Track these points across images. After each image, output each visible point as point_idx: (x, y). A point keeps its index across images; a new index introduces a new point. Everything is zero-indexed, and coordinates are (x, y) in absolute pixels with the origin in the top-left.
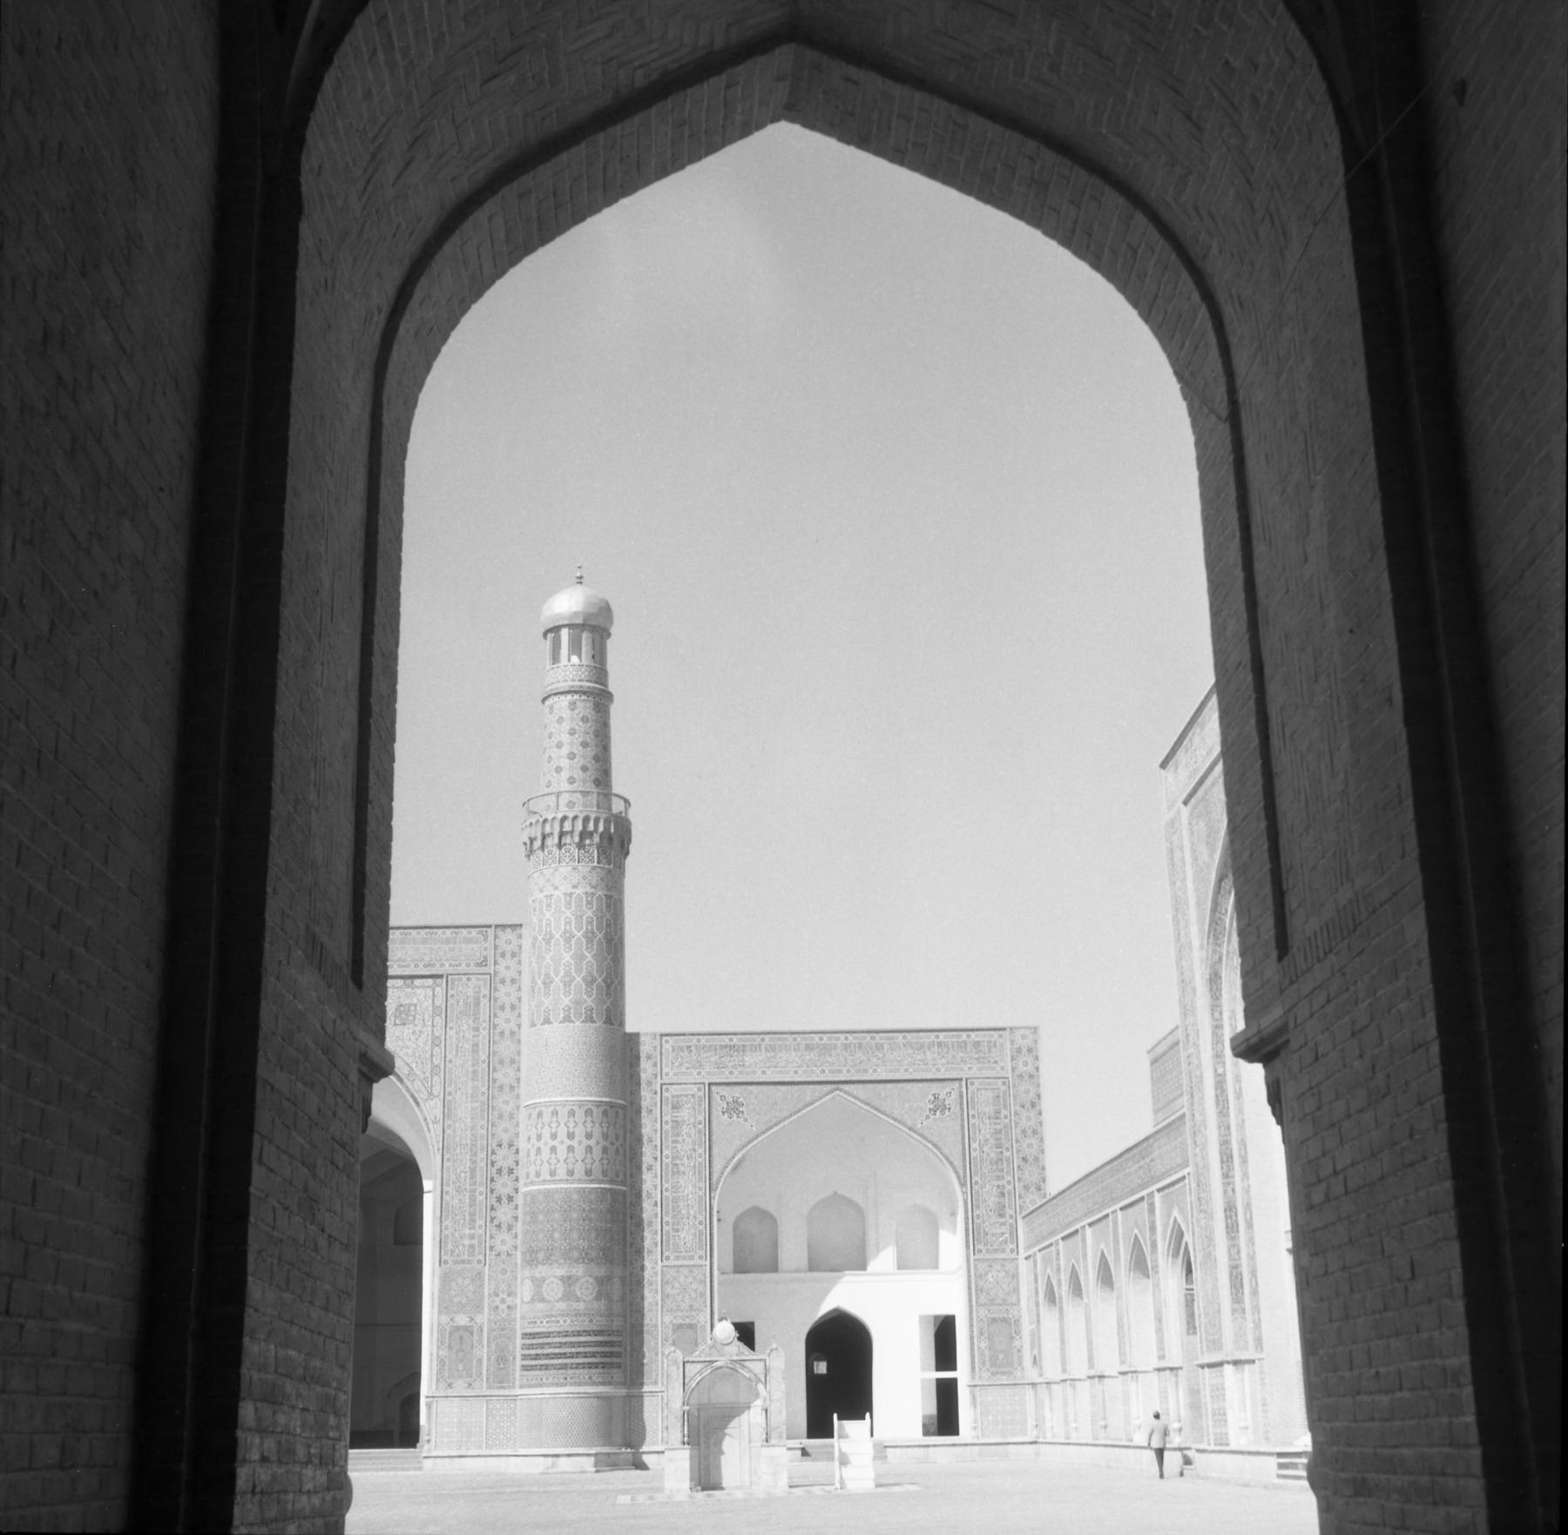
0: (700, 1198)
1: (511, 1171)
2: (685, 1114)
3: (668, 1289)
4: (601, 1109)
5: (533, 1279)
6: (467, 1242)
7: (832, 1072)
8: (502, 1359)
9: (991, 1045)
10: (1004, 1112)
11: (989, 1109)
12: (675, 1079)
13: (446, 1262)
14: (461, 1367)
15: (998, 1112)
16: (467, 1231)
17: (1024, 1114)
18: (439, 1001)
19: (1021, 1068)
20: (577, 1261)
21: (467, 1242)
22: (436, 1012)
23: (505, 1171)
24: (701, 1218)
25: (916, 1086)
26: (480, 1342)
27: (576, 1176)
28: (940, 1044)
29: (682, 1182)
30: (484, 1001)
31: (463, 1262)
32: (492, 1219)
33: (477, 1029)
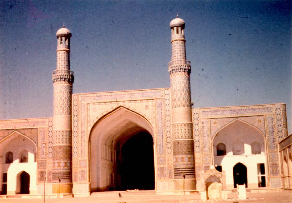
0: (209, 141)
1: (170, 137)
2: (205, 125)
3: (203, 159)
4: (187, 124)
5: (175, 158)
6: (162, 151)
7: (236, 115)
8: (170, 173)
9: (270, 108)
10: (274, 122)
11: (271, 121)
12: (203, 118)
13: (158, 155)
14: (162, 175)
15: (272, 122)
16: (162, 149)
17: (278, 122)
18: (154, 104)
19: (277, 113)
20: (184, 154)
21: (162, 151)
22: (153, 106)
23: (169, 137)
24: (209, 145)
25: (254, 117)
26: (166, 170)
27: (183, 138)
28: (259, 108)
29: (205, 138)
30: (163, 104)
31: (162, 155)
32: (167, 146)
33: (161, 109)
